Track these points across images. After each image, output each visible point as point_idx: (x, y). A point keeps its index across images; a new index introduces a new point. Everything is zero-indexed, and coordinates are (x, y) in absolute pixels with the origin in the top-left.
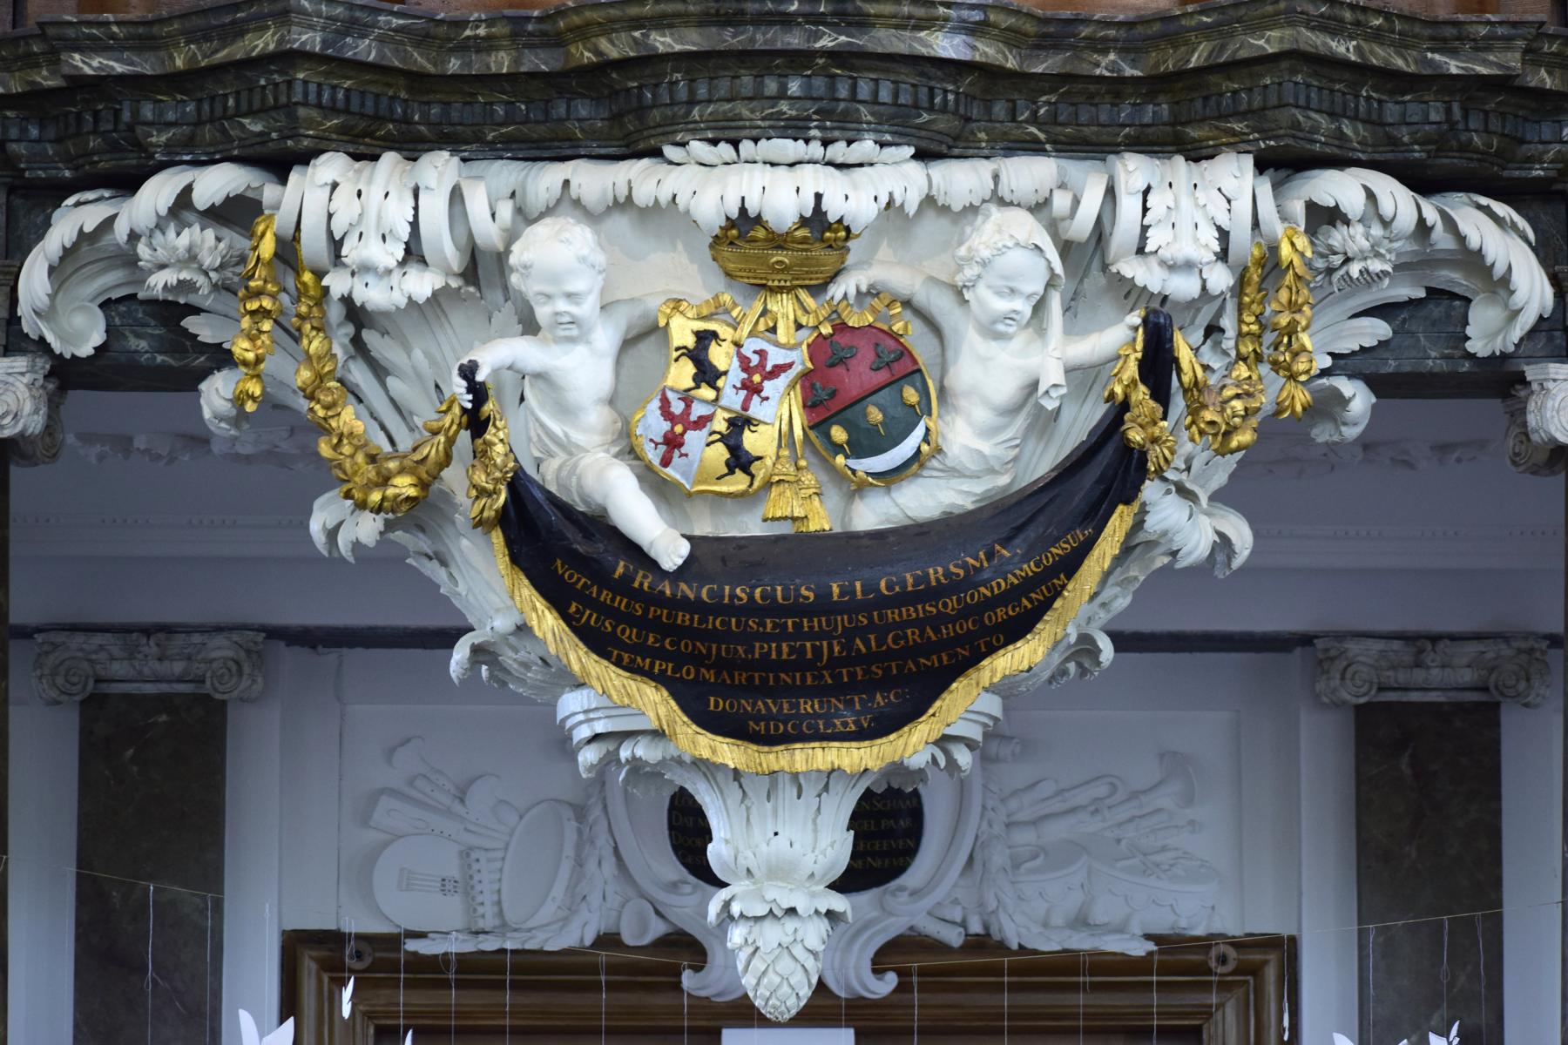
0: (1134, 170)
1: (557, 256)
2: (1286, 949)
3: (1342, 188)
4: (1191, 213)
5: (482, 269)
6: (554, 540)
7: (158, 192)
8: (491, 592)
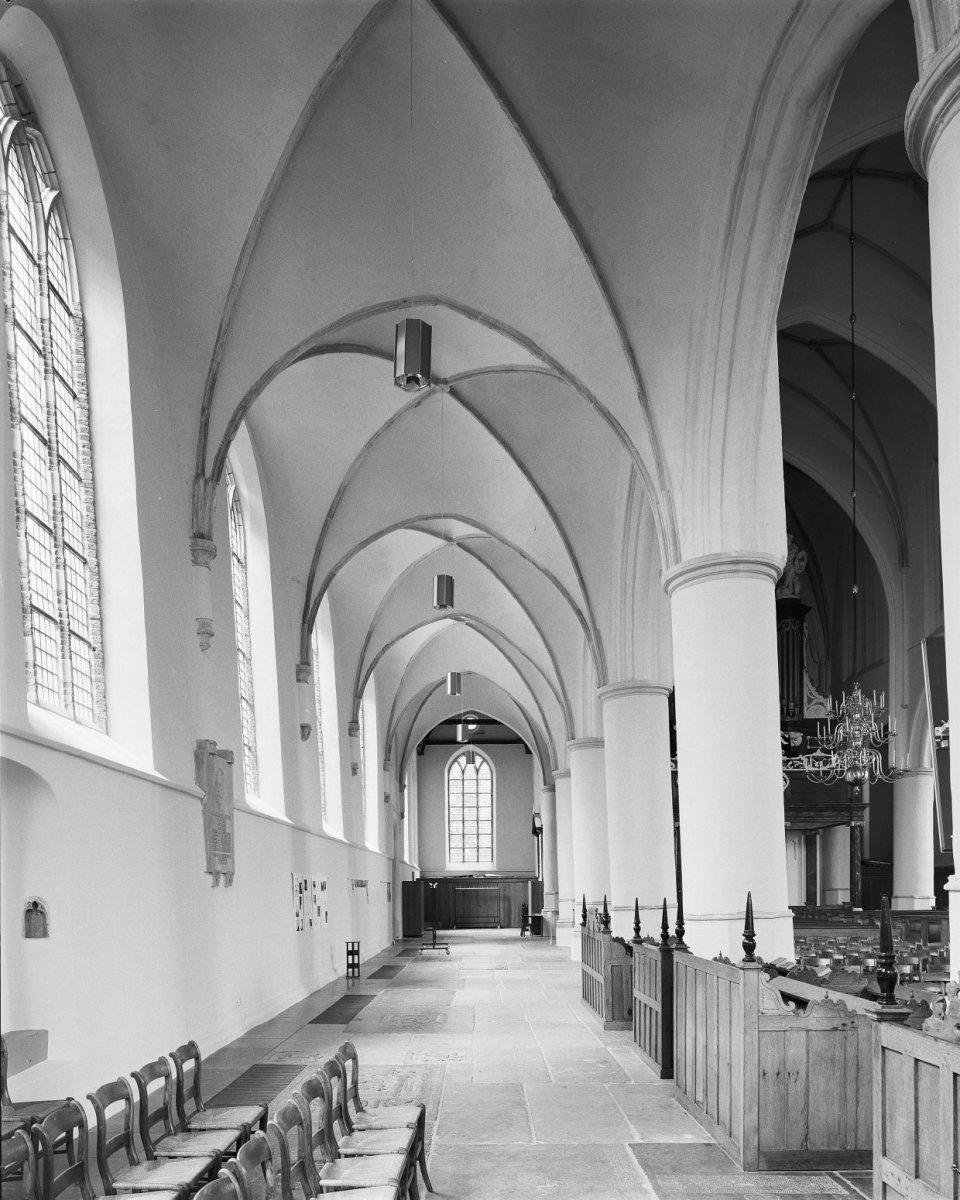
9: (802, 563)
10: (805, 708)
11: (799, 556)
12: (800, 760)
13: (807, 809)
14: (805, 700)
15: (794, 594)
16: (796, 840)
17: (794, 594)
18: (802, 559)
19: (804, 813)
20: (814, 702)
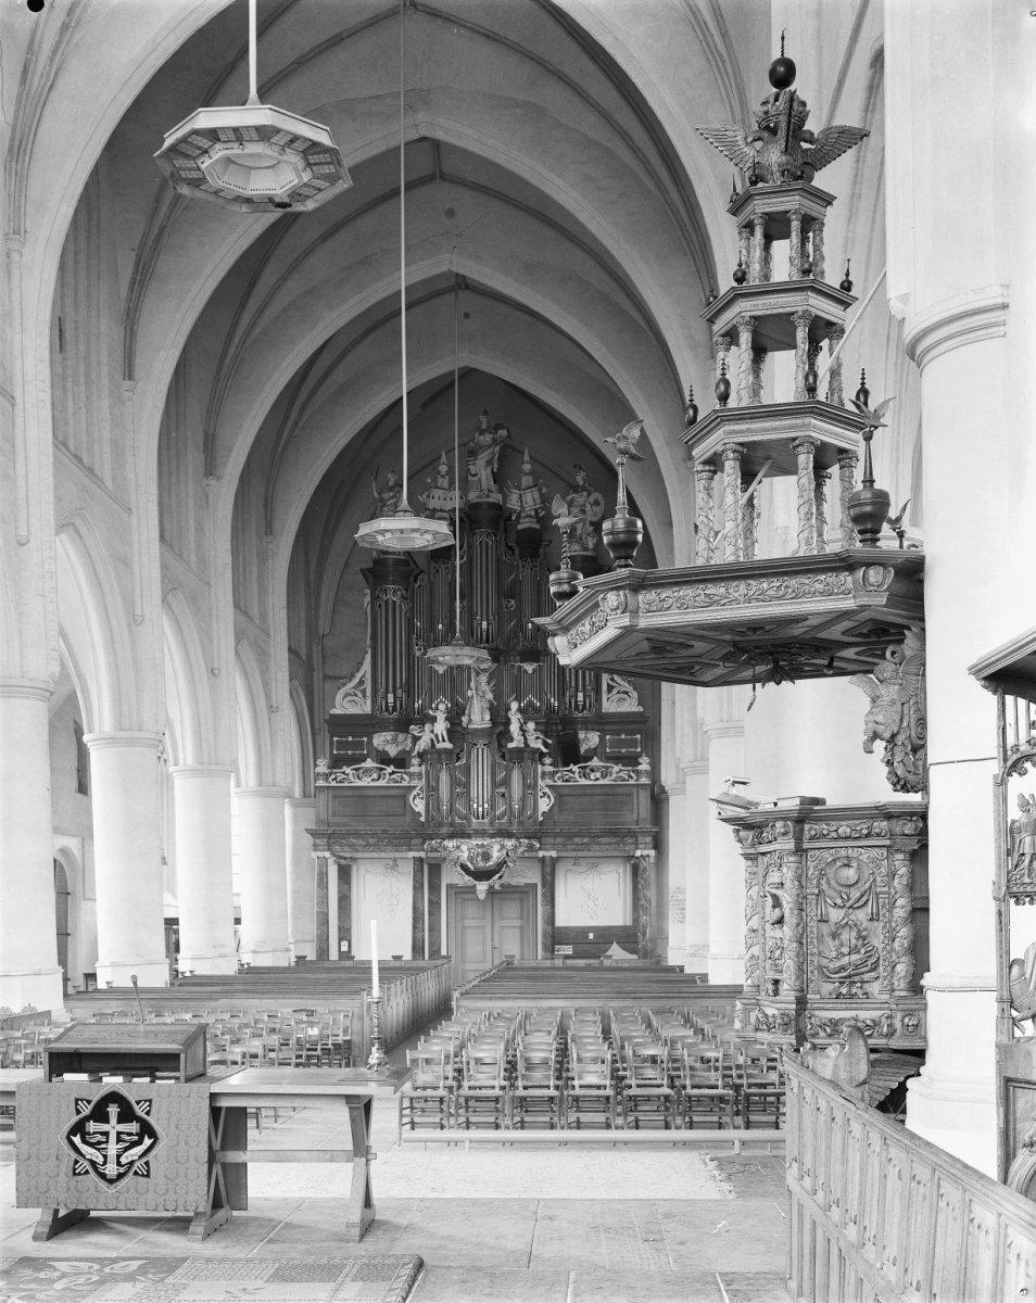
0: (506, 840)
1: (464, 848)
2: (536, 885)
3: (522, 840)
4: (509, 843)
5: (458, 847)
6: (464, 867)
7: (434, 842)
8: (459, 868)
9: (596, 509)
10: (604, 696)
11: (591, 499)
12: (570, 771)
13: (579, 834)
14: (604, 688)
15: (586, 549)
16: (621, 871)
17: (586, 549)
18: (596, 503)
19: (576, 840)
20: (614, 692)
